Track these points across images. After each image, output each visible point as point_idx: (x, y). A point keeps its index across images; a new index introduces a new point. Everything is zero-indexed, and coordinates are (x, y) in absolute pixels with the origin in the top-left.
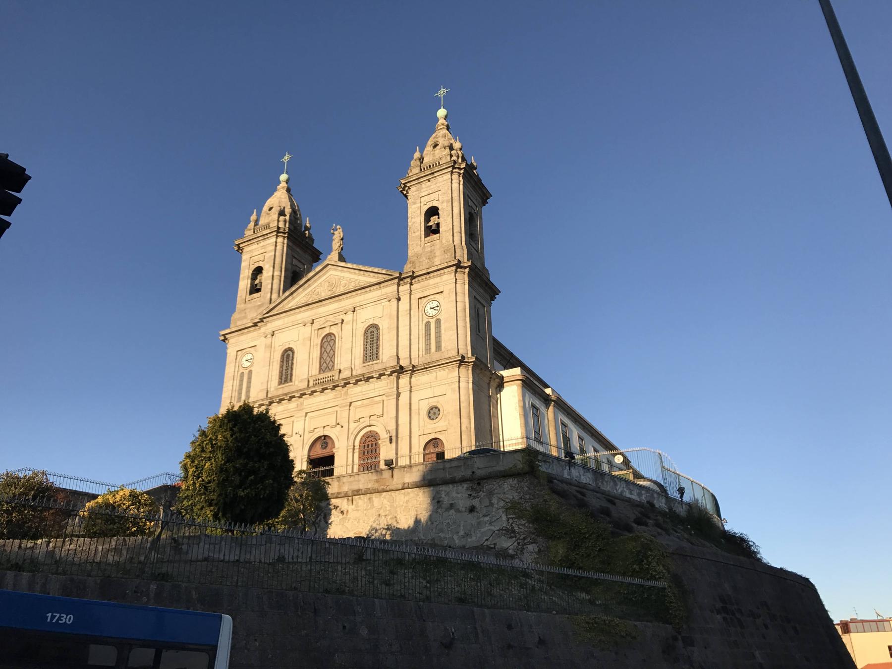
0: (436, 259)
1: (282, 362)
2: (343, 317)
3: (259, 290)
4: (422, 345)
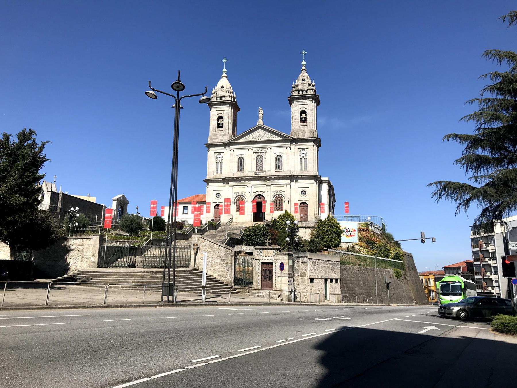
1: (239, 162)
3: (222, 127)
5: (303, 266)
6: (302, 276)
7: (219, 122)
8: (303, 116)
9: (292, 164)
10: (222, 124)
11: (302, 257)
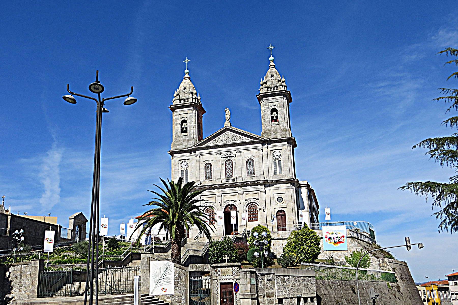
0: (278, 134)
2: (235, 153)
3: (186, 132)
4: (273, 171)
5: (269, 285)
6: (268, 297)
7: (183, 127)
8: (274, 114)
9: (266, 169)
10: (186, 128)
11: (267, 274)
